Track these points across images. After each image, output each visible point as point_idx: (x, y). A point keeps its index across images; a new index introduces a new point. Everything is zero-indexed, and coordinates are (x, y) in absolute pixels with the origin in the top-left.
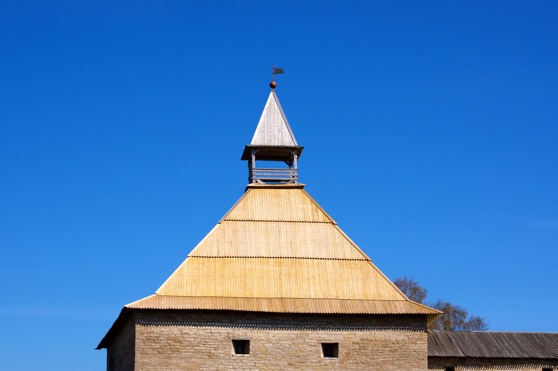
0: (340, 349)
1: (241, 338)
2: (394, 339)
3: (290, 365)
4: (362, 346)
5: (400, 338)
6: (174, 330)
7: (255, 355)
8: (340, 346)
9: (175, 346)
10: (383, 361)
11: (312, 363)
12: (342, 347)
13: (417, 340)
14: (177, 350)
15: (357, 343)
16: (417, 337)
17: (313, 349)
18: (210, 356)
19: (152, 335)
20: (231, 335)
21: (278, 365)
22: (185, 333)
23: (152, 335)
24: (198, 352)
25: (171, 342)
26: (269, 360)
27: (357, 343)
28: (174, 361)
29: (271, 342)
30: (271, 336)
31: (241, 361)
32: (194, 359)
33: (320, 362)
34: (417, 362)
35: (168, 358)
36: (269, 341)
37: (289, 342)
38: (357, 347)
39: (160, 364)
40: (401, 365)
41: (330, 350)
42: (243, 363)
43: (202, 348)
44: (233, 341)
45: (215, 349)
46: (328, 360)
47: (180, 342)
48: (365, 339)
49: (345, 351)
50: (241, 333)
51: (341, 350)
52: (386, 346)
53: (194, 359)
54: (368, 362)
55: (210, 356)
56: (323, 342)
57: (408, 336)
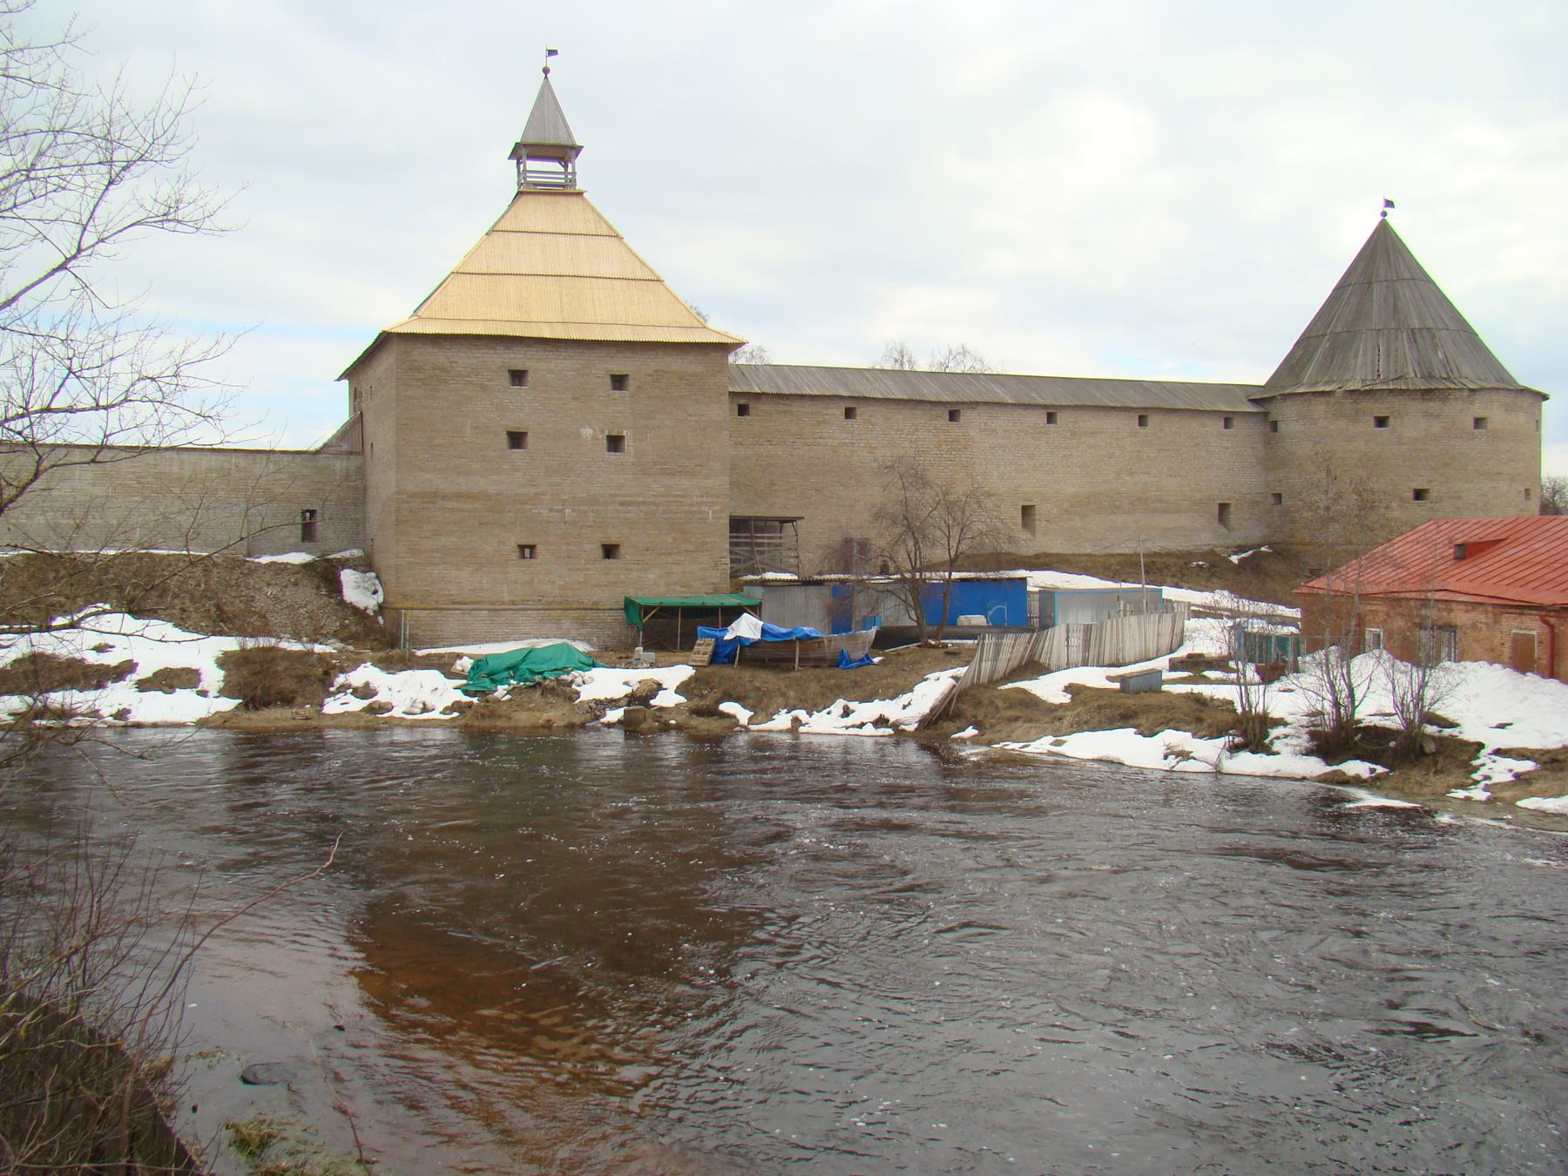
3: (575, 399)
6: (440, 356)
18: (483, 388)
36: (551, 372)
41: (619, 381)
46: (617, 393)
50: (518, 359)
51: (632, 384)
52: (681, 378)
55: (483, 388)
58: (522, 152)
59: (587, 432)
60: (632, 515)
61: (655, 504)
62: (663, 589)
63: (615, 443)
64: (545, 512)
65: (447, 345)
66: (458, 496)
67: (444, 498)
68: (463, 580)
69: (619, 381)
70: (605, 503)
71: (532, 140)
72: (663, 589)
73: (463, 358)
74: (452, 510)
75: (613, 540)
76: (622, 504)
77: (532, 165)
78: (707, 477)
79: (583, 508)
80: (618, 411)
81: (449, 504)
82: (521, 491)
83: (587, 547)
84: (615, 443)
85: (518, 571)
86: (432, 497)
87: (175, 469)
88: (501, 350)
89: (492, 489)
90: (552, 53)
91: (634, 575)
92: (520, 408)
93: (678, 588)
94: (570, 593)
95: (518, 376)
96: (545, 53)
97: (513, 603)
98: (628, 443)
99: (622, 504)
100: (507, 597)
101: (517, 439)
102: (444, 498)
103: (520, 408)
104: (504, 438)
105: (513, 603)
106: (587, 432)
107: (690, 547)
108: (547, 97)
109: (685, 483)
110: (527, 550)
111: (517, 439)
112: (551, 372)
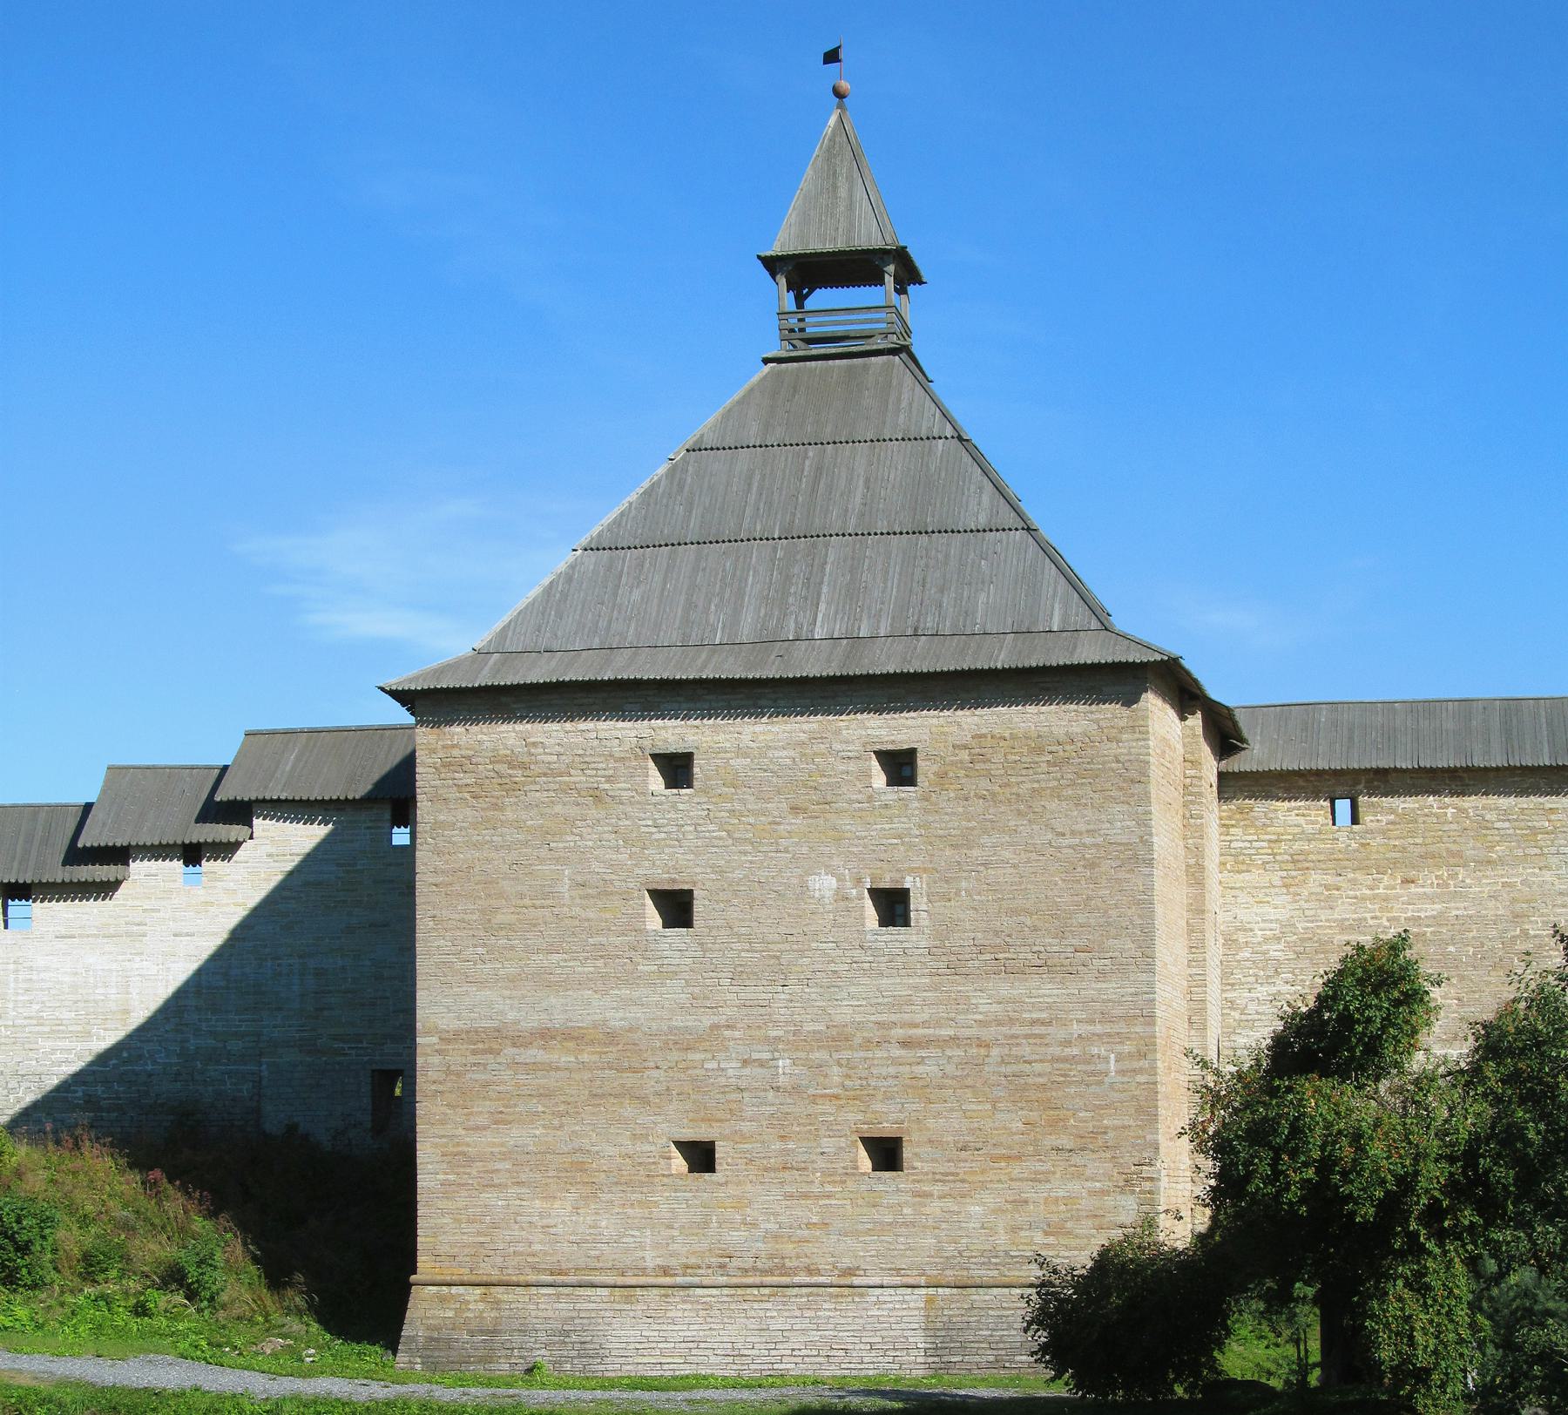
0: (922, 764)
1: (672, 750)
2: (1059, 732)
3: (795, 809)
4: (978, 751)
5: (1076, 729)
6: (506, 736)
9: (514, 775)
10: (1034, 790)
11: (850, 802)
12: (928, 758)
13: (1122, 730)
14: (512, 788)
15: (965, 747)
16: (1122, 723)
17: (852, 767)
18: (597, 797)
19: (456, 752)
20: (647, 743)
21: (764, 813)
22: (534, 744)
23: (456, 752)
24: (567, 789)
25: (502, 768)
26: (744, 802)
27: (965, 747)
28: (510, 814)
29: (746, 756)
30: (746, 739)
31: (674, 806)
32: (558, 809)
33: (870, 799)
34: (1121, 789)
35: (495, 807)
36: (740, 752)
37: (792, 753)
38: (964, 755)
39: (475, 825)
40: (1080, 798)
41: (900, 766)
42: (677, 810)
43: (577, 778)
44: (655, 757)
45: (609, 779)
48: (984, 736)
49: (935, 768)
50: (672, 733)
52: (1039, 750)
53: (558, 809)
54: (994, 794)
55: (597, 797)
56: (878, 747)
57: (1097, 721)
59: (824, 884)
60: (928, 1070)
61: (982, 1044)
62: (1002, 1239)
63: (893, 906)
64: (732, 1067)
66: (545, 1036)
67: (519, 1041)
68: (558, 1224)
69: (900, 766)
70: (867, 1044)
72: (1002, 1239)
74: (534, 1068)
75: (886, 1129)
76: (905, 1044)
77: (822, 298)
78: (1102, 975)
79: (819, 1055)
81: (535, 1054)
82: (678, 1022)
83: (828, 1144)
84: (893, 906)
89: (617, 1019)
90: (832, 57)
91: (934, 1208)
93: (1039, 1238)
94: (789, 1248)
95: (677, 769)
97: (666, 1271)
98: (917, 903)
99: (905, 1044)
100: (651, 1259)
102: (519, 1041)
103: (683, 837)
105: (666, 1271)
107: (1066, 1142)
109: (1048, 991)
111: (676, 907)
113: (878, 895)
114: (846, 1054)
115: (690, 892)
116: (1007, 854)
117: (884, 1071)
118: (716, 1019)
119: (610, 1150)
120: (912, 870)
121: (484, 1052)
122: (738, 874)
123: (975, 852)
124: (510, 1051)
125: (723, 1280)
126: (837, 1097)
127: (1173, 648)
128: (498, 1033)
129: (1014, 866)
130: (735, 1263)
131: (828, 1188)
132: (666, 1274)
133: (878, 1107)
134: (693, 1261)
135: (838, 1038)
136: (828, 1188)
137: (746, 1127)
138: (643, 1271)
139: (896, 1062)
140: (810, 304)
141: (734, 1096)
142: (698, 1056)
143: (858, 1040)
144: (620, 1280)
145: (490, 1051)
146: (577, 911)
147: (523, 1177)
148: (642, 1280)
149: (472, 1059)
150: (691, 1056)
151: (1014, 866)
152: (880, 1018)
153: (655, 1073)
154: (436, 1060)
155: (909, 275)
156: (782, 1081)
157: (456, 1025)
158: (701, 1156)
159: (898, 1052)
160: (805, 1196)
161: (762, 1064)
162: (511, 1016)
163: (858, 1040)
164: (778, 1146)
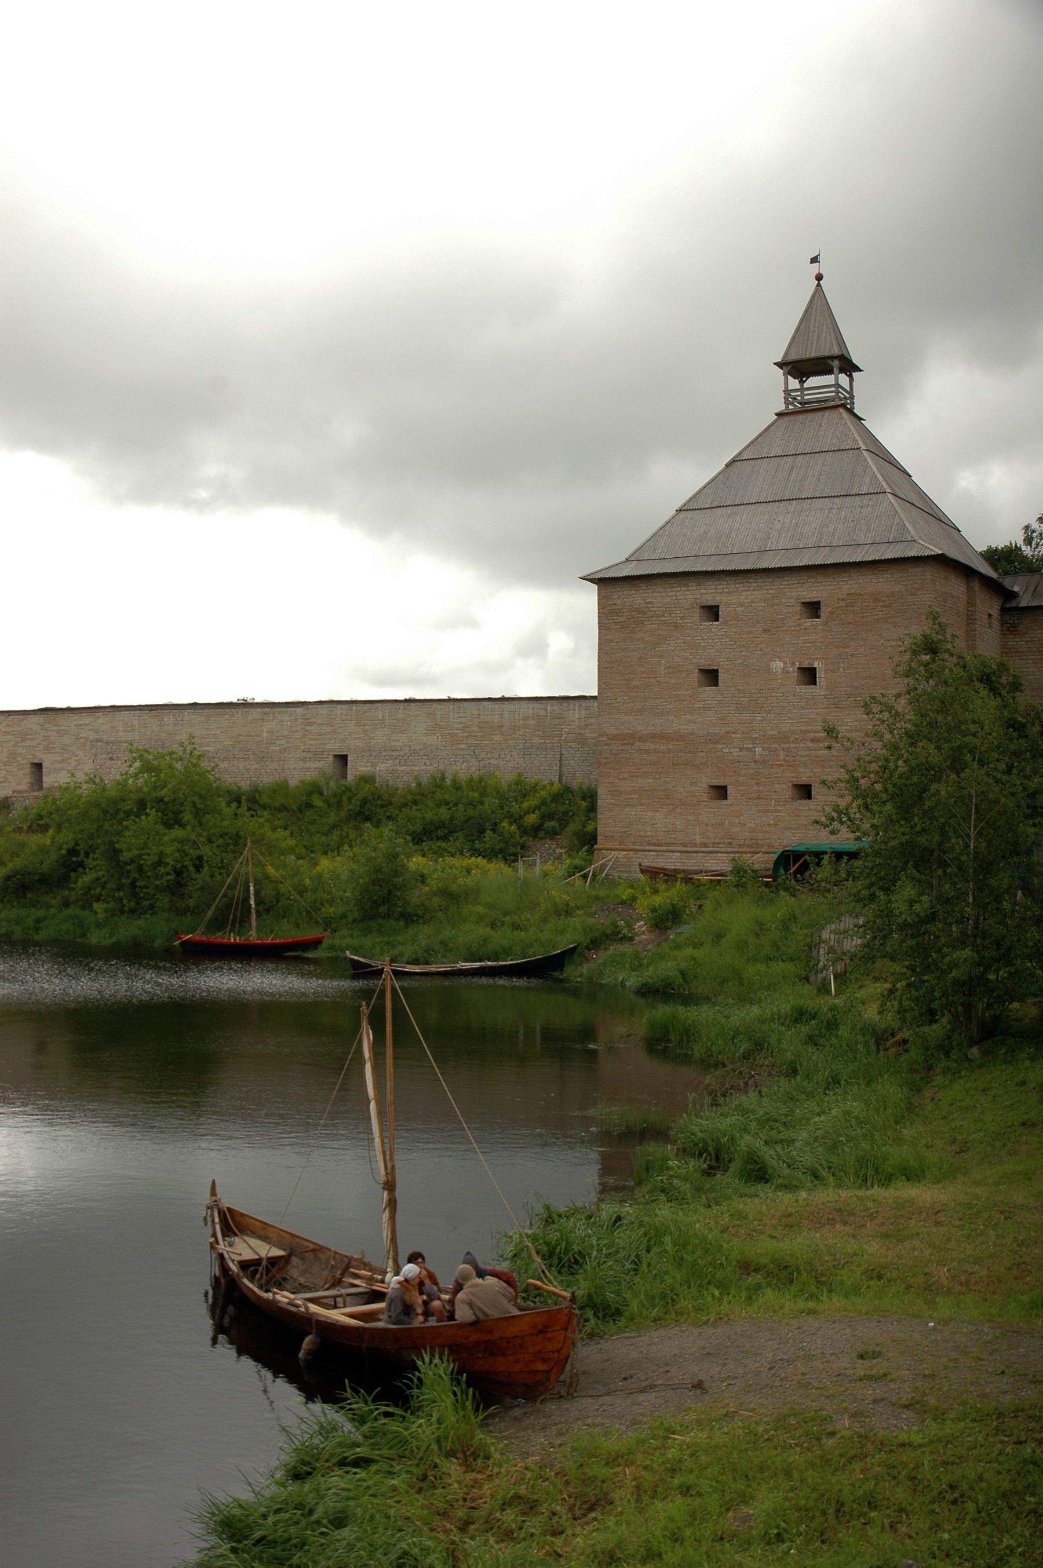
1: (709, 604)
3: (765, 631)
7: (725, 623)
8: (822, 604)
17: (791, 610)
18: (677, 627)
21: (751, 632)
22: (650, 603)
24: (665, 622)
25: (635, 614)
36: (741, 605)
38: (842, 604)
41: (813, 608)
46: (809, 623)
47: (644, 613)
51: (824, 611)
55: (677, 627)
58: (798, 367)
59: (777, 665)
63: (809, 675)
65: (643, 586)
66: (653, 737)
67: (641, 739)
71: (793, 357)
73: (657, 597)
74: (648, 752)
75: (804, 780)
77: (813, 381)
80: (811, 641)
81: (646, 746)
83: (777, 787)
85: (712, 811)
86: (632, 738)
87: (496, 718)
88: (693, 585)
89: (685, 729)
90: (815, 260)
92: (712, 644)
94: (760, 836)
96: (821, 259)
97: (705, 845)
99: (812, 741)
100: (698, 840)
101: (711, 676)
102: (641, 739)
103: (712, 644)
104: (695, 675)
105: (705, 845)
106: (777, 665)
108: (818, 310)
110: (721, 792)
111: (711, 676)
112: (741, 605)
113: (802, 670)
114: (787, 745)
115: (717, 671)
116: (862, 650)
117: (803, 753)
118: (728, 729)
119: (681, 789)
120: (817, 659)
121: (625, 744)
122: (739, 661)
123: (847, 650)
124: (637, 744)
125: (729, 850)
126: (782, 765)
127: (161, 520)
128: (633, 736)
129: (865, 656)
130: (735, 842)
131: (778, 808)
132: (705, 847)
133: (800, 770)
134: (717, 841)
135: (783, 738)
136: (778, 808)
137: (741, 779)
138: (695, 845)
139: (809, 749)
140: (806, 385)
141: (737, 765)
142: (720, 746)
143: (792, 738)
144: (684, 849)
145: (629, 744)
146: (667, 679)
147: (643, 802)
148: (695, 849)
149: (621, 748)
150: (717, 746)
151: (865, 656)
152: (803, 728)
153: (702, 754)
154: (606, 748)
155: (849, 367)
156: (757, 757)
157: (615, 732)
158: (721, 792)
159: (810, 744)
160: (768, 811)
161: (748, 749)
162: (638, 728)
163: (792, 738)
164: (755, 787)
